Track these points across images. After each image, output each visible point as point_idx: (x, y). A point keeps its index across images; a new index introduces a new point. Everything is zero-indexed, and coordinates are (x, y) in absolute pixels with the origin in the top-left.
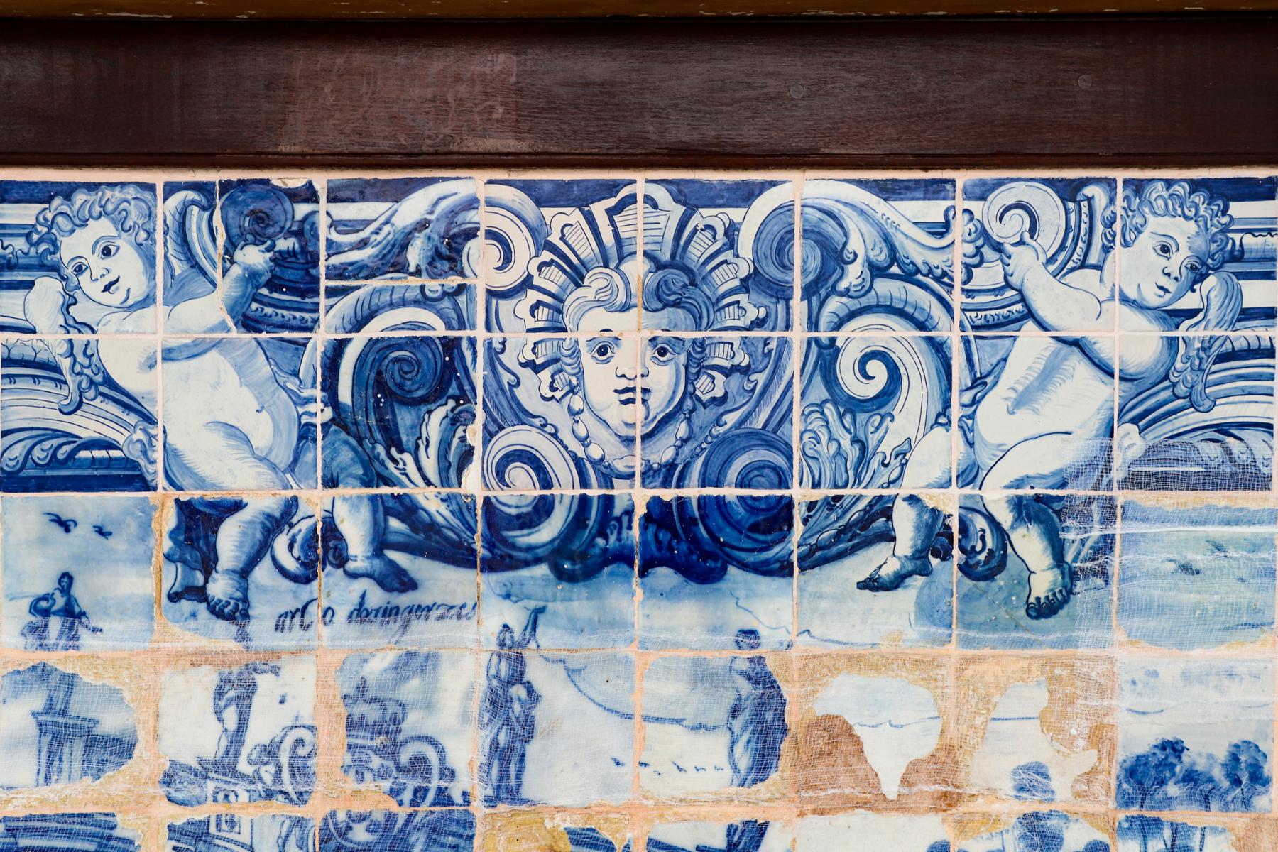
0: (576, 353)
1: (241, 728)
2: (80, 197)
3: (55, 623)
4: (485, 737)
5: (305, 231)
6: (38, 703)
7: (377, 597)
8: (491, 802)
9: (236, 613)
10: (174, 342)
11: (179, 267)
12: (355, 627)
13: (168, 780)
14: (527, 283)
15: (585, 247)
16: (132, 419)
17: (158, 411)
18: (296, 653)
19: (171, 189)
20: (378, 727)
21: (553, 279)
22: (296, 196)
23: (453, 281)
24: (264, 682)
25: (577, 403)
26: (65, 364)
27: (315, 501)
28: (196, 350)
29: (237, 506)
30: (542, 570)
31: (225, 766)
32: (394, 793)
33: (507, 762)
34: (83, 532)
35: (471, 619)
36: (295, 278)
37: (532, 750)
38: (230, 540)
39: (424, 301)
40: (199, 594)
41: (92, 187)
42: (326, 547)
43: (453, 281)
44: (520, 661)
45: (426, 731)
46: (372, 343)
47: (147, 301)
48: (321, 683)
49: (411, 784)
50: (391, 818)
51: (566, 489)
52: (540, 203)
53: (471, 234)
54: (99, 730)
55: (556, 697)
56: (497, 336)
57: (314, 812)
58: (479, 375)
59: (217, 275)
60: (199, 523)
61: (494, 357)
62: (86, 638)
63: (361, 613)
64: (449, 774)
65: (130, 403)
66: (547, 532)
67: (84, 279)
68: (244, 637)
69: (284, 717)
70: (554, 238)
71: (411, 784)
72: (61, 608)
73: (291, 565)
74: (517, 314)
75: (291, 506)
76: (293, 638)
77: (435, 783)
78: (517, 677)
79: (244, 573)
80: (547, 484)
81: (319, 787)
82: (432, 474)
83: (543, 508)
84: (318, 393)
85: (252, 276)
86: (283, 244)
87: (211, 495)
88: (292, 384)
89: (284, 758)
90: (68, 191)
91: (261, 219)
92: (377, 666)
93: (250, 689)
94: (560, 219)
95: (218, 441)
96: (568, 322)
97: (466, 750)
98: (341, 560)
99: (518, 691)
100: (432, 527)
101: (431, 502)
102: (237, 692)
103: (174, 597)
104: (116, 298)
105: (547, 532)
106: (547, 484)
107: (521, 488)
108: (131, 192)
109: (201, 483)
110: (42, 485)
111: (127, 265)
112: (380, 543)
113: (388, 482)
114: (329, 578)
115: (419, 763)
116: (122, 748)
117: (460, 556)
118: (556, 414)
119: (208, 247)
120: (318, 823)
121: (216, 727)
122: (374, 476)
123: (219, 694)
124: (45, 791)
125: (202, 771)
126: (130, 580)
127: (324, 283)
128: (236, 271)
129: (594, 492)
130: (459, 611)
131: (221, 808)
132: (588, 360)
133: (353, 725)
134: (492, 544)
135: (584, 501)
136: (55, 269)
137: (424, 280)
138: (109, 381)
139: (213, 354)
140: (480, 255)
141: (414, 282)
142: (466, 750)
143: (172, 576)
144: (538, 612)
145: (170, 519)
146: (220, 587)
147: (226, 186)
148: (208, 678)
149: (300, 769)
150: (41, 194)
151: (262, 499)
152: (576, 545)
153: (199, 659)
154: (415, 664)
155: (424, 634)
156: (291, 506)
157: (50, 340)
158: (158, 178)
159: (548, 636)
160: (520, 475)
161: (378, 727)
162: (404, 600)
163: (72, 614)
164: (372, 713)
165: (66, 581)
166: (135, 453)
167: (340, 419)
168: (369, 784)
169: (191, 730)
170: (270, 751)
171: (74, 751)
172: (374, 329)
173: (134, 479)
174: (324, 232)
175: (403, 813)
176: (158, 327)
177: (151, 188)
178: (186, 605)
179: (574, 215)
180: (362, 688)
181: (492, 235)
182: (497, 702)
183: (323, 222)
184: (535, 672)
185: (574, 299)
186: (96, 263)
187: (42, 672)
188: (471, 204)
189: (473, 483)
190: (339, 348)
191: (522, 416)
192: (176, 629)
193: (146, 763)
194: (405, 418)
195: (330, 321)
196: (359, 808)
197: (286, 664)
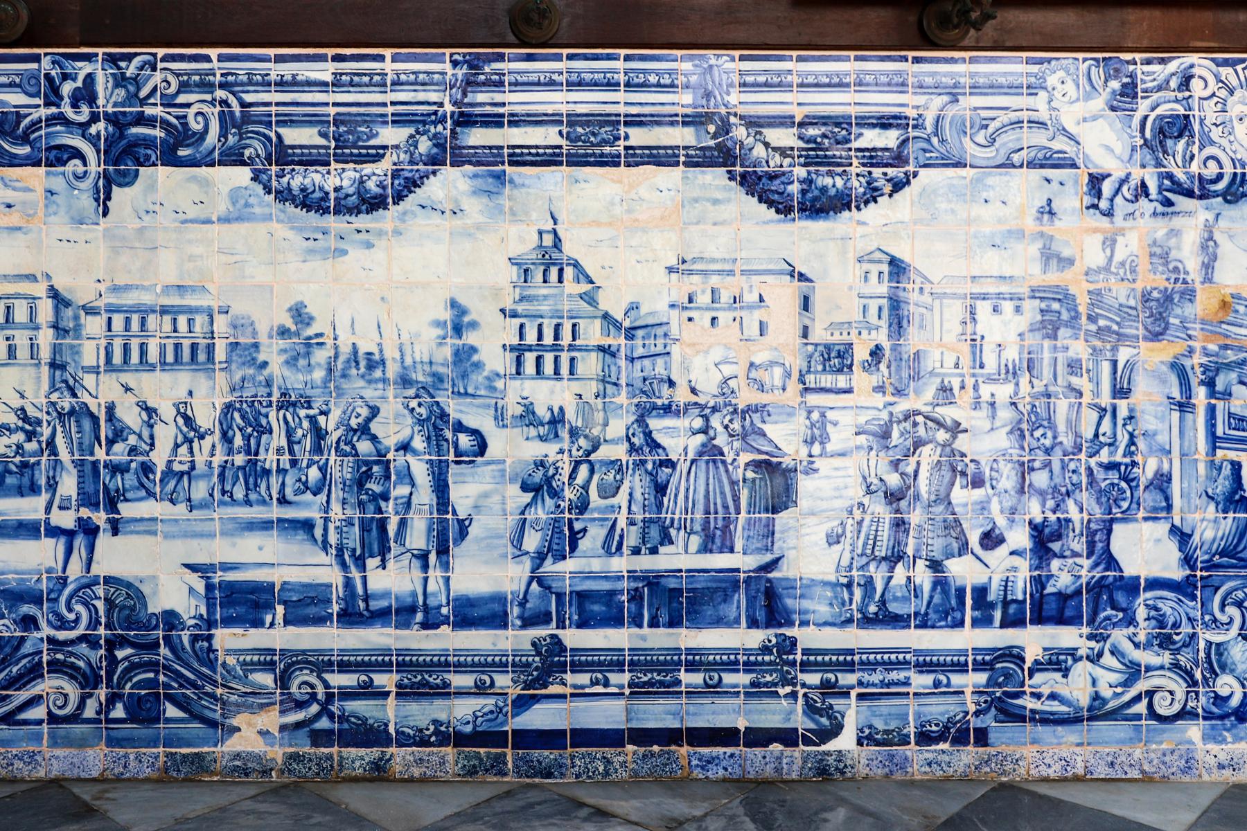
0: (1231, 120)
1: (1112, 256)
2: (1053, 63)
3: (1046, 217)
4: (1200, 260)
5: (1132, 76)
6: (1040, 245)
7: (1160, 208)
8: (1203, 283)
9: (1109, 214)
10: (1087, 116)
11: (1088, 88)
12: (1152, 219)
13: (1087, 274)
14: (1214, 95)
15: (1234, 81)
16: (1072, 143)
17: (1081, 141)
18: (1130, 229)
19: (1085, 60)
20: (1161, 256)
21: (1223, 93)
22: (1128, 62)
23: (1187, 94)
24: (1120, 239)
25: (1232, 138)
26: (1049, 123)
27: (1137, 174)
28: (1094, 118)
29: (1109, 175)
30: (1220, 199)
31: (1107, 269)
32: (1168, 279)
33: (1208, 268)
34: (1055, 184)
35: (1195, 217)
36: (1130, 91)
37: (1217, 265)
38: (1107, 187)
39: (1177, 101)
40: (1095, 206)
41: (1057, 59)
42: (1143, 188)
43: (1187, 94)
44: (1211, 232)
45: (1179, 257)
46: (1158, 116)
47: (1078, 99)
48: (1140, 240)
49: (1173, 276)
50: (1166, 289)
51: (1228, 170)
52: (1218, 65)
53: (1192, 76)
54: (1062, 255)
55: (1226, 247)
56: (1202, 114)
57: (1139, 286)
58: (1196, 127)
59: (1101, 90)
60: (1096, 181)
61: (1202, 121)
62: (1057, 222)
63: (1155, 214)
64: (1187, 273)
65: (1071, 137)
66: (1221, 186)
67: (1055, 92)
68: (1112, 223)
69: (1127, 252)
70: (1223, 78)
71: (1173, 276)
72: (1048, 211)
73: (1129, 197)
74: (1210, 105)
75: (1129, 174)
76: (1130, 223)
77: (1182, 276)
78: (1211, 238)
79: (1112, 200)
80: (1221, 168)
81: (1140, 277)
82: (1180, 164)
83: (1220, 177)
84: (1138, 134)
85: (1114, 92)
86: (1126, 80)
87: (1100, 171)
88: (1129, 131)
89: (1127, 267)
90: (1049, 61)
91: (1117, 70)
92: (1160, 234)
93: (1114, 241)
94: (1225, 72)
95: (1102, 151)
96: (1228, 108)
97: (1192, 264)
98: (1147, 195)
99: (1211, 243)
100: (1179, 184)
101: (1180, 175)
102: (1110, 243)
103: (1088, 208)
104: (1066, 99)
105: (1221, 186)
106: (1221, 168)
107: (1212, 170)
108: (1071, 61)
109: (1096, 166)
110: (1042, 166)
111: (1070, 87)
112: (1161, 189)
113: (1164, 167)
114: (1143, 201)
115: (1176, 269)
116: (1071, 262)
117: (1189, 194)
118: (1224, 142)
119: (1098, 81)
120: (1140, 290)
121: (1102, 255)
122: (1159, 164)
123: (1104, 243)
124: (1044, 277)
125: (1099, 271)
126: (1071, 199)
127: (1140, 94)
128: (1108, 90)
129: (1239, 171)
130: (1189, 214)
131: (1105, 284)
132: (1236, 123)
133: (1152, 255)
134: (1201, 190)
135: (1235, 174)
136: (1045, 88)
137: (1176, 93)
138: (1064, 129)
139: (1101, 120)
140: (1196, 84)
141: (1173, 94)
142: (1192, 264)
143: (1087, 200)
144: (1218, 215)
145: (1086, 179)
146: (1104, 204)
147: (1104, 59)
148: (1100, 237)
149: (1133, 271)
150: (1040, 62)
151: (1119, 174)
152: (1233, 190)
153: (1096, 230)
154: (1174, 233)
155: (1177, 222)
156: (1129, 174)
157: (1044, 115)
158: (1081, 56)
159: (1222, 223)
160: (1211, 164)
161: (1161, 256)
162: (1170, 210)
163: (1051, 213)
164: (1158, 251)
165: (1050, 201)
166: (1073, 156)
167: (1146, 143)
168: (1158, 276)
169: (1094, 255)
170: (1123, 264)
171: (1054, 262)
172: (1159, 111)
173: (1074, 166)
174: (1139, 76)
175: (1170, 287)
176: (1080, 109)
177: (1077, 59)
178: (1092, 211)
179: (1230, 70)
180: (1155, 242)
181: (1200, 77)
182: (1204, 247)
183: (1139, 73)
184: (1217, 236)
185: (1230, 100)
186: (1059, 86)
187: (1042, 234)
188: (1192, 66)
189: (1195, 168)
190: (1146, 117)
191: (1212, 143)
192: (1088, 219)
193: (1078, 267)
194: (1169, 143)
195: (1143, 106)
196: (1154, 285)
197: (1127, 232)
